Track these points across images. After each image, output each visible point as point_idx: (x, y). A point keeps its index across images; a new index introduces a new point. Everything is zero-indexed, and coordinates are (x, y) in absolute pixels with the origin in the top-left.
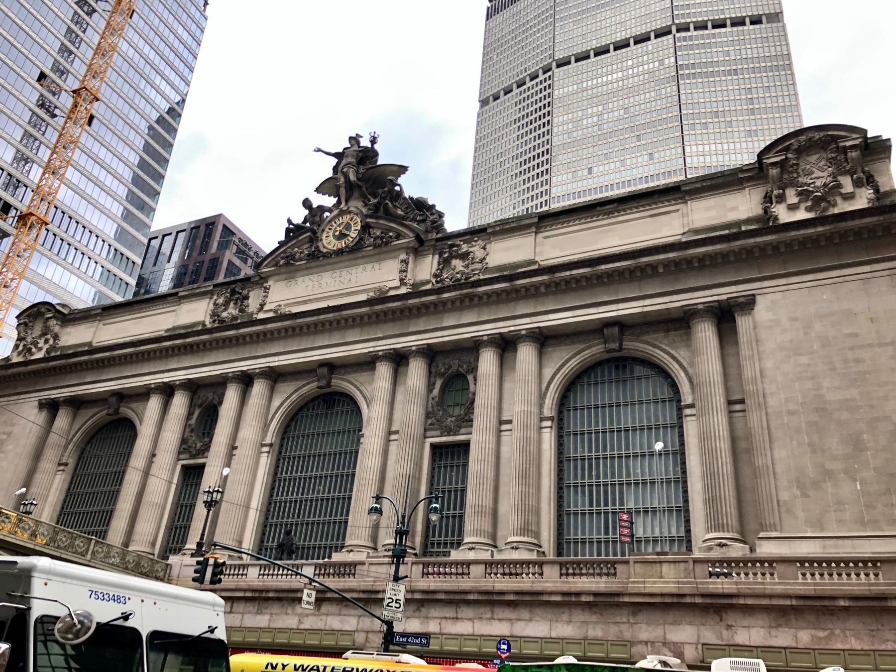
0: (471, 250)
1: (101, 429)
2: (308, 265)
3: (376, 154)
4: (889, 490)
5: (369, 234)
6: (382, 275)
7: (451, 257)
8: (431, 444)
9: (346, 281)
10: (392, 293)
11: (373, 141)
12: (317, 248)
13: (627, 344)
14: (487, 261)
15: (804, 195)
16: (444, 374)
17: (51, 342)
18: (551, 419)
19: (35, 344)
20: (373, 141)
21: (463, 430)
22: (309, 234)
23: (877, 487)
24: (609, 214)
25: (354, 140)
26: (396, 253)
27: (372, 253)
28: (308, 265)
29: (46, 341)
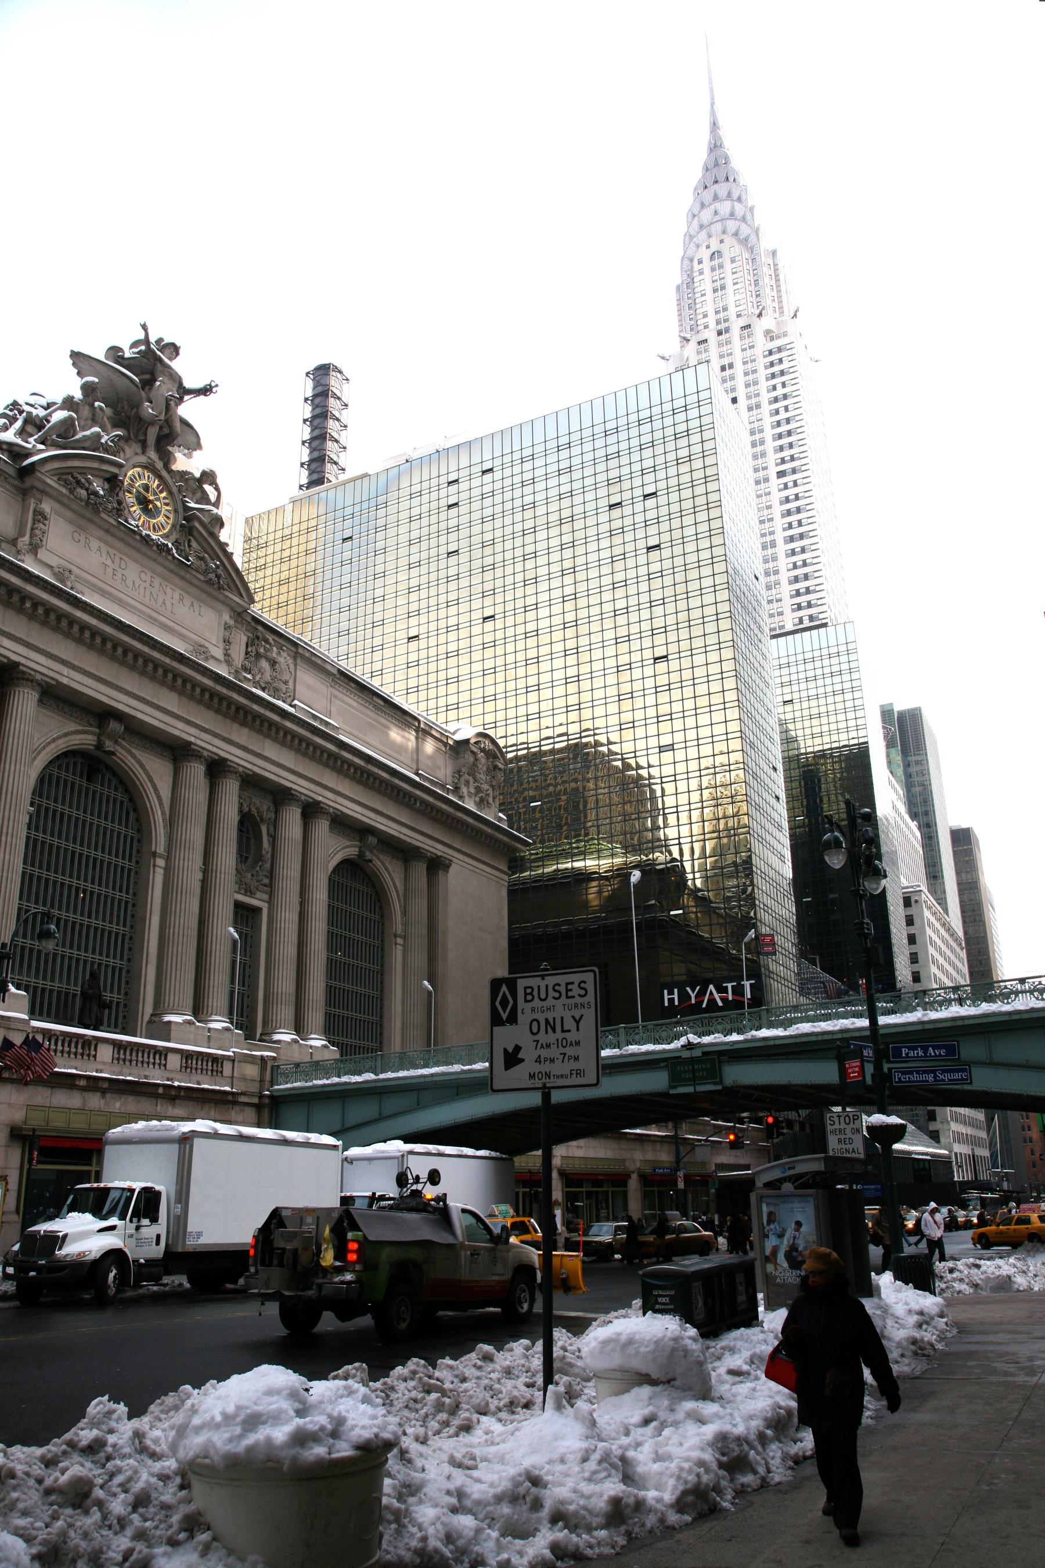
0: (281, 660)
2: (112, 529)
5: (190, 546)
9: (160, 602)
11: (206, 391)
12: (120, 503)
15: (478, 790)
20: (206, 391)
21: (258, 895)
22: (115, 470)
26: (220, 606)
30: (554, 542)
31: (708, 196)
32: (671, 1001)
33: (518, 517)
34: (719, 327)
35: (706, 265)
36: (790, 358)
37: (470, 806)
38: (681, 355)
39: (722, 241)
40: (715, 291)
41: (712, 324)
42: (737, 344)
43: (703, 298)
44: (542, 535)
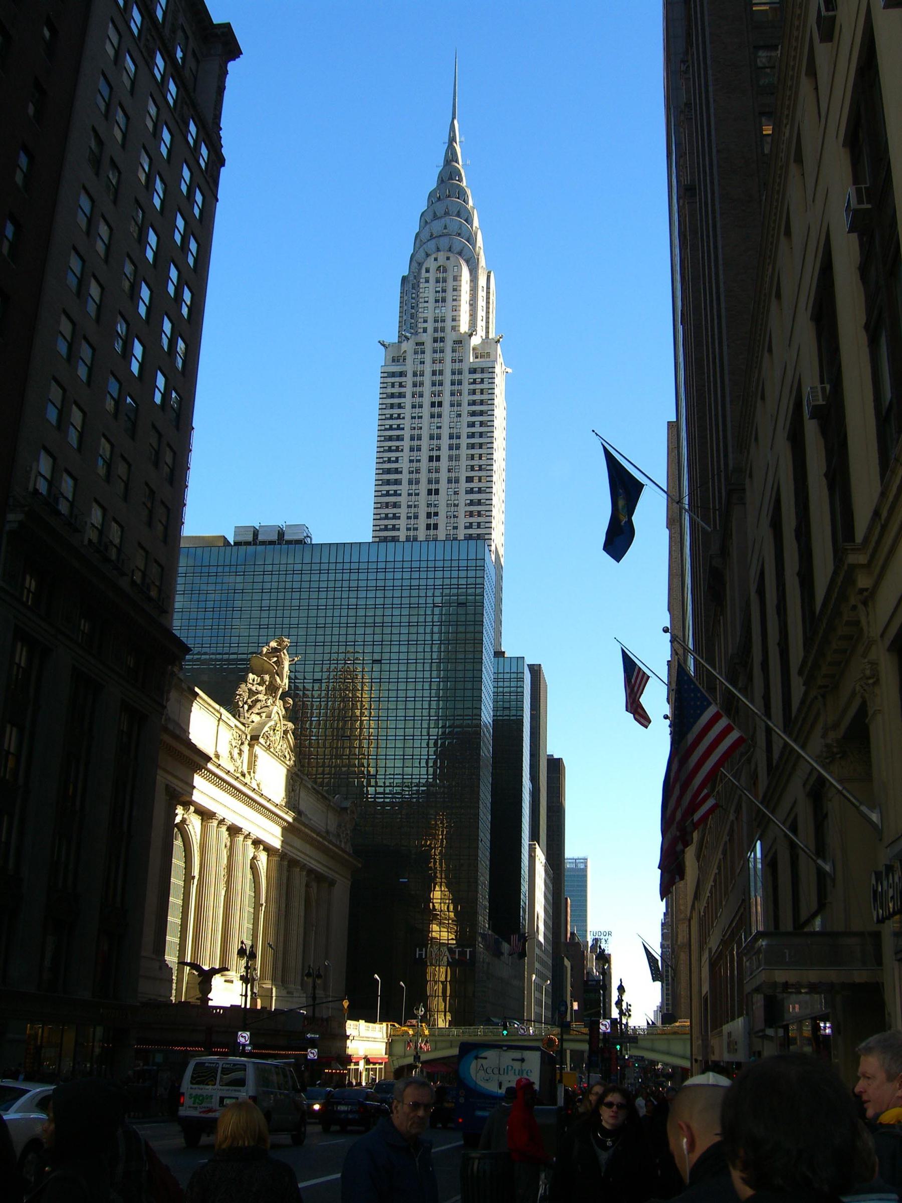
30: (369, 638)
31: (440, 208)
32: (421, 955)
33: (344, 612)
34: (436, 335)
35: (432, 276)
36: (490, 381)
37: (343, 845)
38: (399, 348)
39: (448, 259)
40: (437, 301)
41: (430, 330)
42: (448, 355)
43: (426, 305)
44: (360, 631)
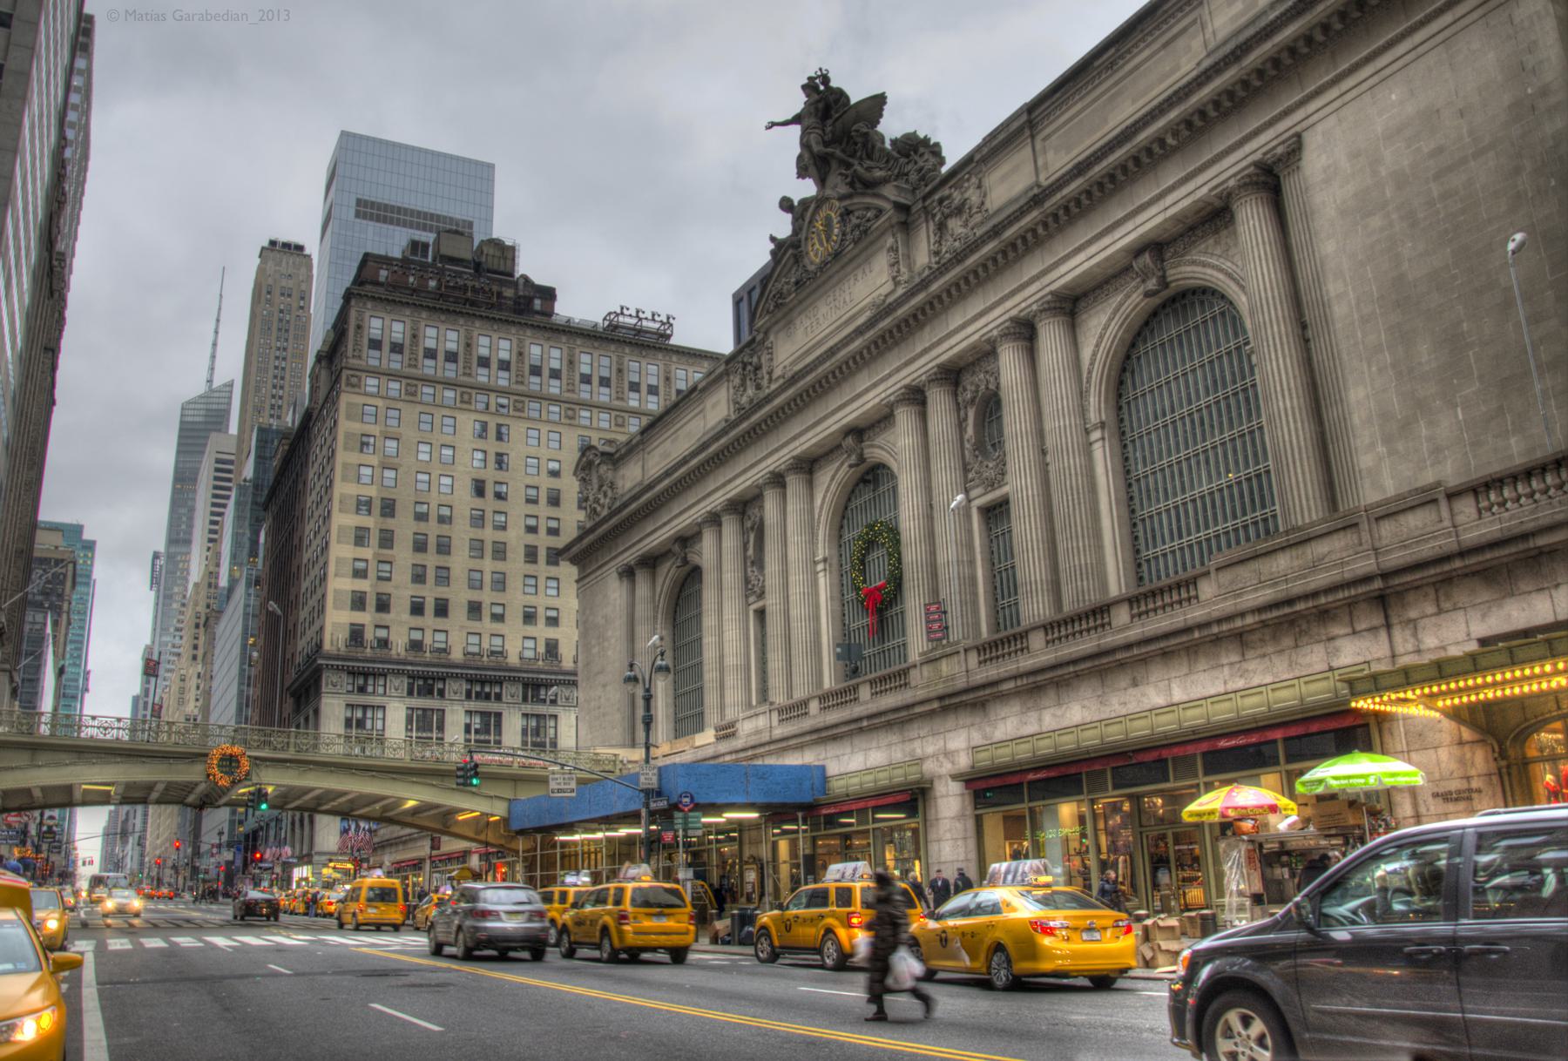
1: (683, 585)
2: (801, 297)
3: (841, 95)
4: (1501, 407)
6: (871, 284)
7: (947, 217)
8: (980, 509)
10: (890, 299)
13: (1172, 274)
14: (988, 205)
16: (973, 400)
17: (610, 493)
18: (1102, 425)
19: (597, 501)
23: (1484, 409)
24: (1111, 66)
25: (810, 87)
27: (856, 251)
28: (801, 297)
29: (605, 495)
